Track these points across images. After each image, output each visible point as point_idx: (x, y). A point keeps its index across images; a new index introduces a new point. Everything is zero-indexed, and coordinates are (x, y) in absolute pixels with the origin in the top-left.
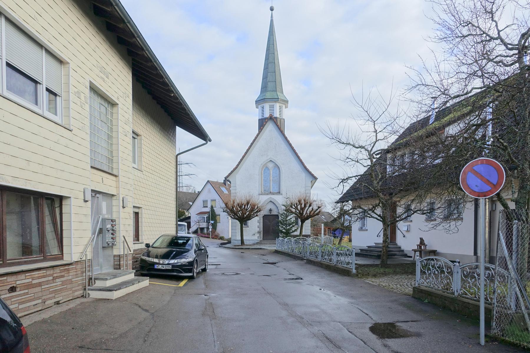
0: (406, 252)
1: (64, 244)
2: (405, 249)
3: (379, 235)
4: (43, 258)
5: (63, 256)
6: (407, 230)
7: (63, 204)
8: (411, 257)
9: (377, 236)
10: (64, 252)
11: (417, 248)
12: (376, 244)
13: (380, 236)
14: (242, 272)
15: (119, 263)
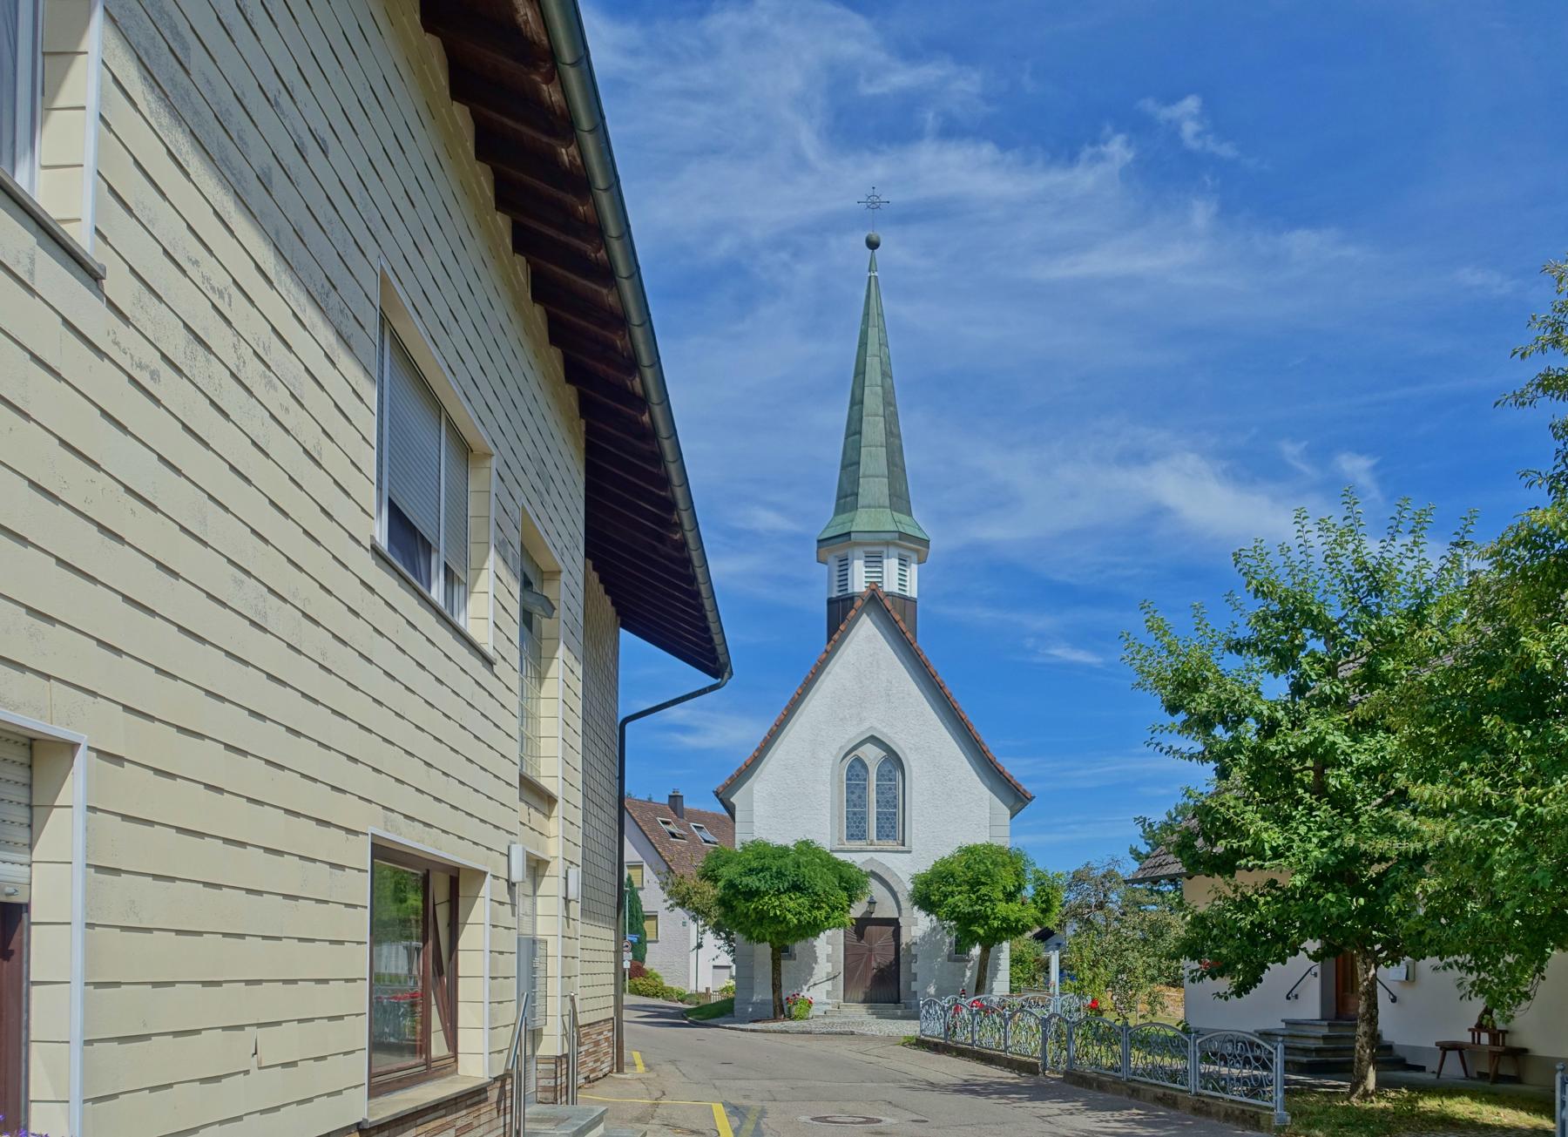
0: (1399, 1053)
1: (462, 1021)
2: (1397, 1043)
3: (1294, 993)
4: (424, 1067)
5: (456, 1061)
6: (1407, 978)
7: (461, 893)
8: (1422, 1069)
9: (1288, 998)
10: (460, 1050)
11: (1470, 1040)
12: (1288, 1023)
13: (1296, 997)
14: (887, 1115)
15: (553, 1084)
